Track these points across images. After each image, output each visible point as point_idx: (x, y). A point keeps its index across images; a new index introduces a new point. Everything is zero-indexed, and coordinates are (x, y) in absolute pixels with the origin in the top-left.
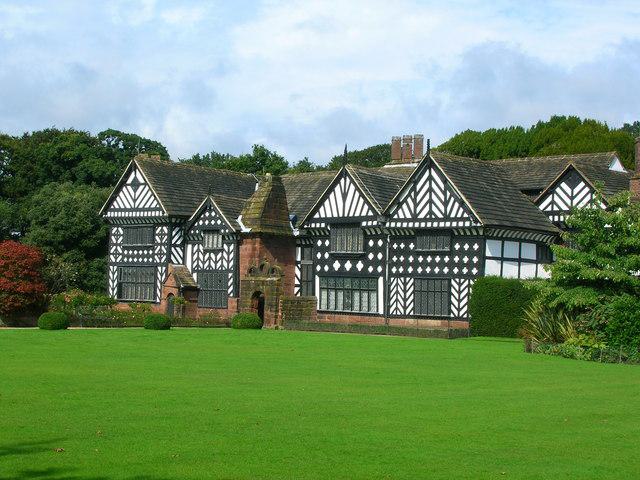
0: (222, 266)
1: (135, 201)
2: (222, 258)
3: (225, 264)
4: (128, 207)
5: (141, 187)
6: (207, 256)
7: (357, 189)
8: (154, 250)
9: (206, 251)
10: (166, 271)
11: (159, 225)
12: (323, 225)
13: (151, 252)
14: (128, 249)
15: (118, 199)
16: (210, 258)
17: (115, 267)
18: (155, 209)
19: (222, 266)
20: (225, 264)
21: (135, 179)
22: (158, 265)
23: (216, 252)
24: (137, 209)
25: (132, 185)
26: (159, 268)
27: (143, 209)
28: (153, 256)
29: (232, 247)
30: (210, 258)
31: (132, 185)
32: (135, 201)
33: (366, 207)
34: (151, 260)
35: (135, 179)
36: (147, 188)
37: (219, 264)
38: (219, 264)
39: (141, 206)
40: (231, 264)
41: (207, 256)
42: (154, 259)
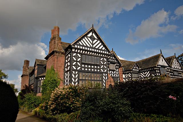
0: (115, 76)
1: (93, 44)
2: (115, 73)
3: (116, 75)
4: (89, 46)
5: (96, 40)
6: (110, 72)
7: (165, 59)
8: (100, 67)
9: (110, 70)
10: (107, 75)
11: (102, 57)
12: (160, 67)
13: (99, 67)
14: (85, 64)
15: (82, 41)
16: (111, 73)
17: (77, 72)
18: (104, 50)
19: (115, 76)
20: (116, 75)
21: (92, 35)
22: (102, 73)
23: (113, 71)
24: (94, 48)
25: (90, 37)
26: (104, 74)
27: (98, 49)
28: (100, 69)
29: (117, 70)
30: (111, 73)
31: (90, 37)
32: (93, 44)
33: (167, 64)
34: (99, 70)
35: (92, 35)
36: (99, 42)
37: (115, 75)
38: (115, 75)
39: (97, 47)
40: (118, 75)
41: (110, 72)
42: (100, 70)
